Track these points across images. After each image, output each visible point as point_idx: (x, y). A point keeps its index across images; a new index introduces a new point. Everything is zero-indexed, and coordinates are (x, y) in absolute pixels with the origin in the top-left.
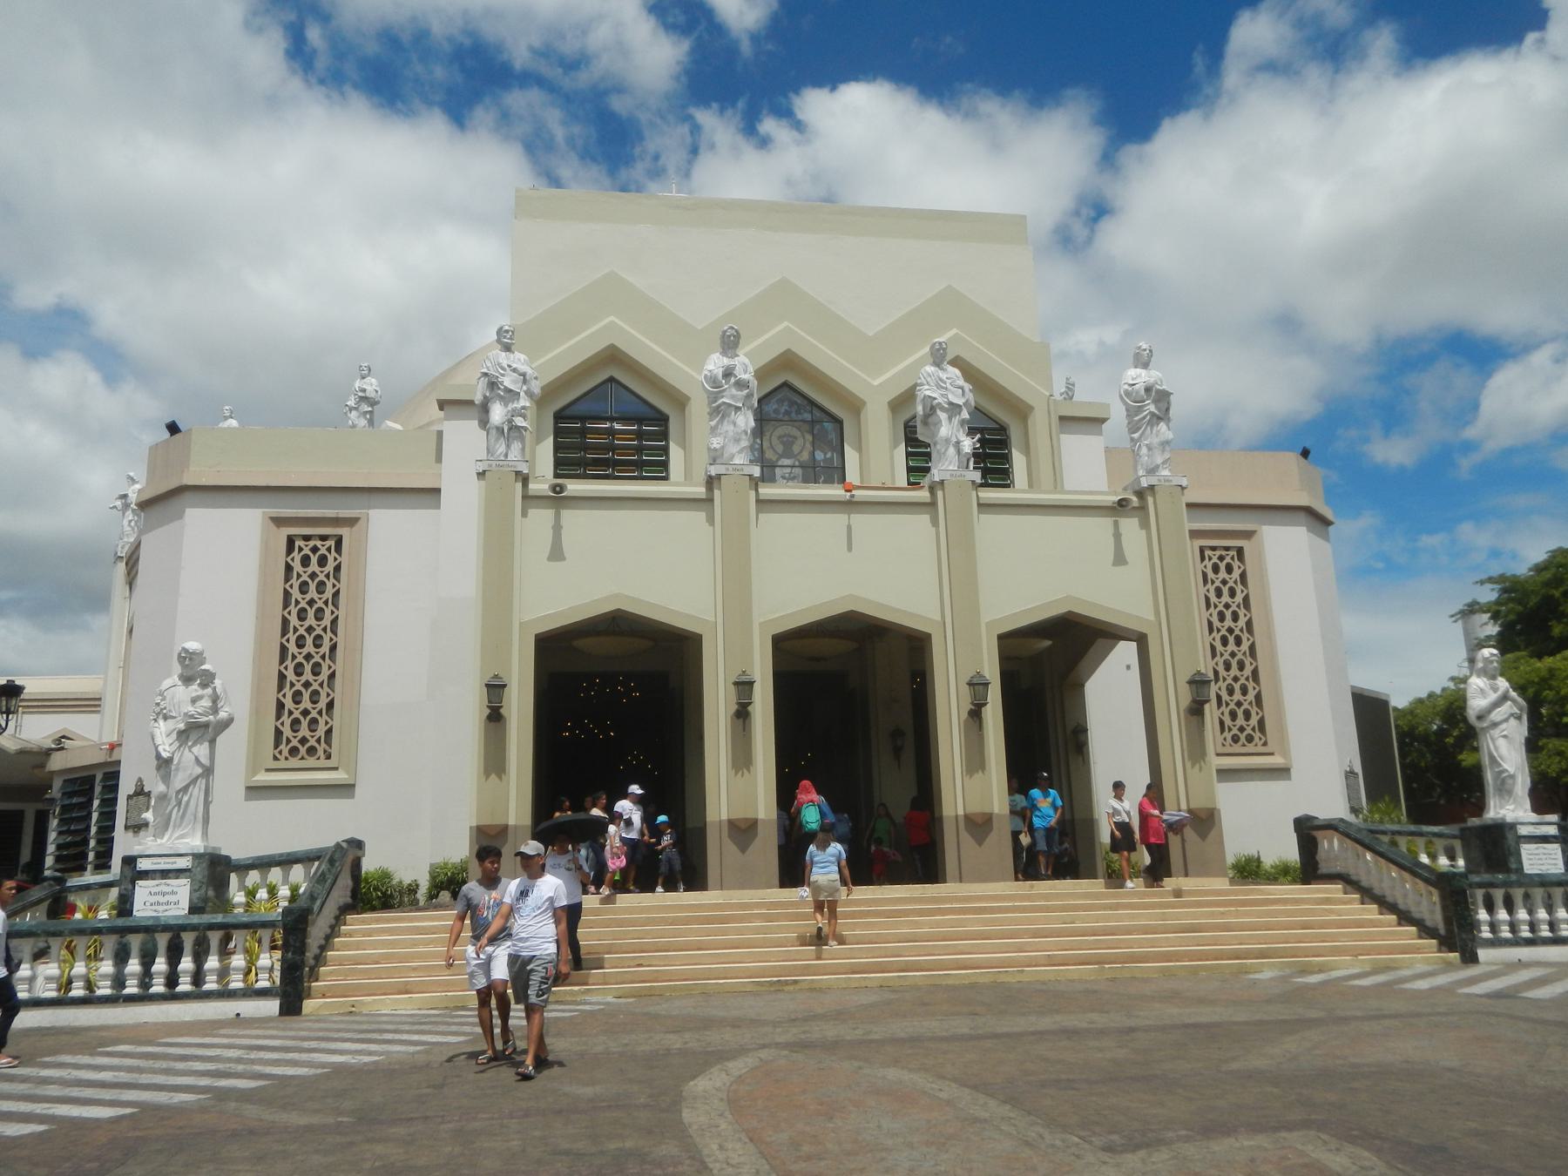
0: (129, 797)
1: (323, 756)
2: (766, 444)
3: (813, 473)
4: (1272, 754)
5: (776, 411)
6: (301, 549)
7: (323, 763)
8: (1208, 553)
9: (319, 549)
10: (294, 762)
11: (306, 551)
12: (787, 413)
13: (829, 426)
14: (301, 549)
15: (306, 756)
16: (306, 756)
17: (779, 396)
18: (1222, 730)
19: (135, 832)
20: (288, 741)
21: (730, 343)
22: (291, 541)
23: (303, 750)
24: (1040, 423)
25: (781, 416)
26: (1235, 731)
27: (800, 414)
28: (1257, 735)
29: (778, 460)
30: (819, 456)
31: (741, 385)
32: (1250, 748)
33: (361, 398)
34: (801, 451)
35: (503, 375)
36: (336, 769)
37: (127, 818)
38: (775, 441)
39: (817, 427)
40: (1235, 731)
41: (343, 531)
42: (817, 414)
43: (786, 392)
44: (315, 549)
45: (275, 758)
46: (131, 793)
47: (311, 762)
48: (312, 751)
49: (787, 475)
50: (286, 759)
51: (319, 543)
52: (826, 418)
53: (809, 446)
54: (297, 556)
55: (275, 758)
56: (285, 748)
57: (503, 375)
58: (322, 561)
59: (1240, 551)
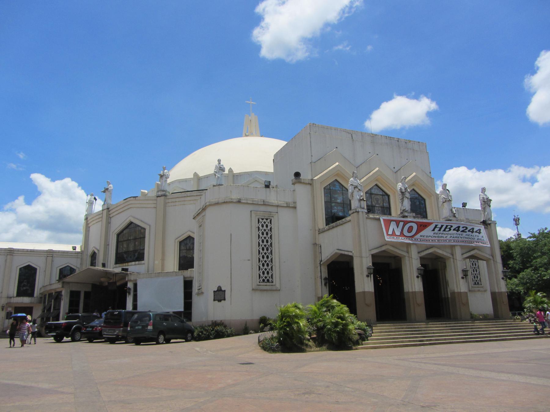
0: (214, 292)
2: (373, 201)
7: (271, 284)
13: (386, 197)
19: (218, 301)
23: (266, 280)
28: (479, 282)
29: (376, 205)
30: (385, 204)
37: (214, 298)
38: (375, 200)
39: (384, 197)
44: (265, 223)
46: (216, 289)
47: (268, 284)
49: (378, 209)
50: (262, 282)
51: (265, 220)
53: (382, 202)
55: (259, 282)
56: (262, 280)
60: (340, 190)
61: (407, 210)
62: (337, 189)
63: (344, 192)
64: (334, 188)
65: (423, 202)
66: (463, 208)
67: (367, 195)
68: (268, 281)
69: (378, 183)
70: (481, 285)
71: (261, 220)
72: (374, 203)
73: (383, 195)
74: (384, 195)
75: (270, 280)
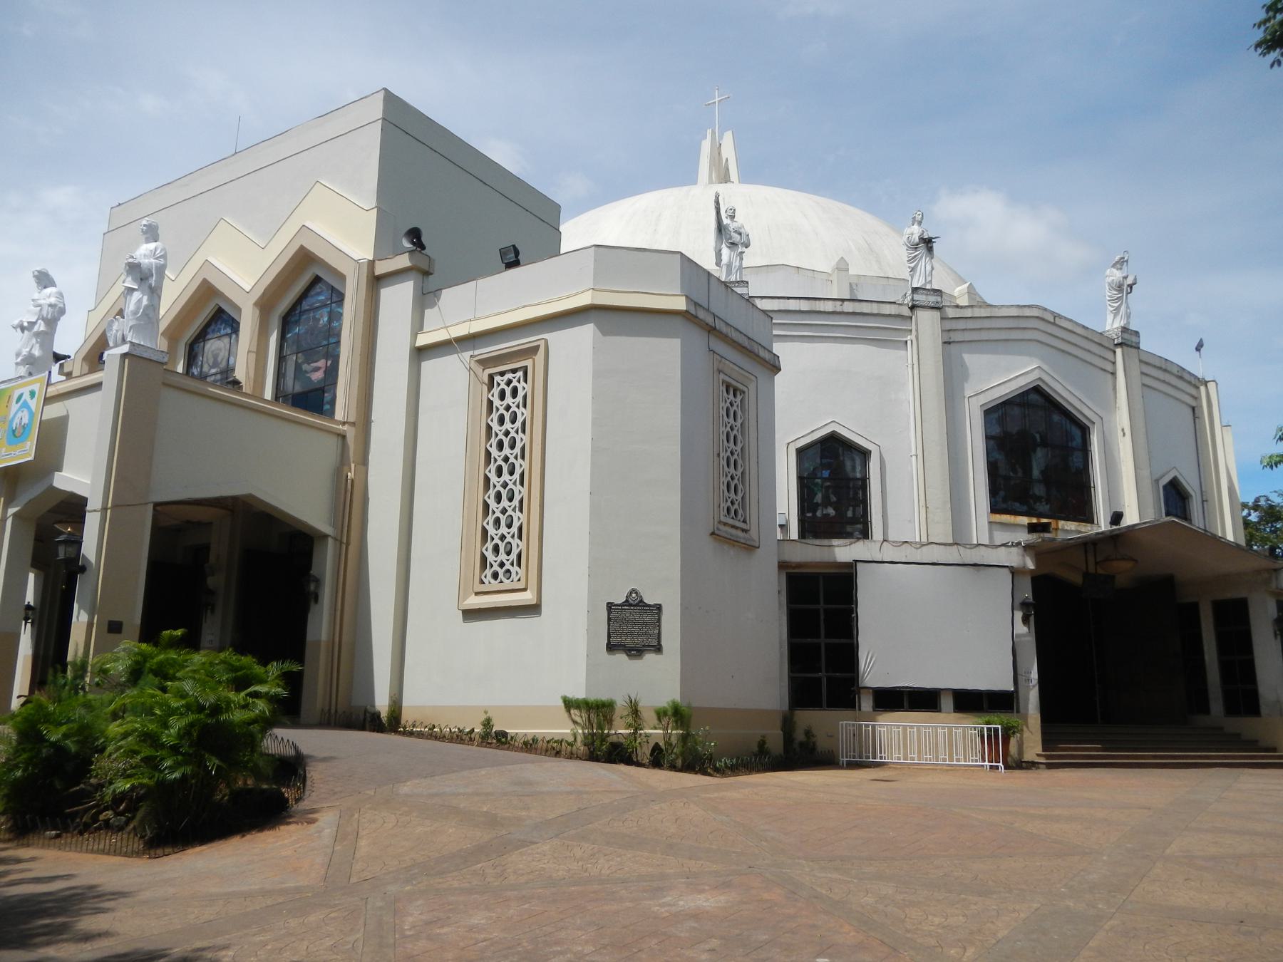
6: (499, 384)
10: (495, 585)
14: (499, 384)
36: (525, 590)
41: (528, 363)
47: (507, 584)
51: (510, 376)
54: (496, 391)
56: (489, 572)
58: (515, 392)
71: (498, 378)
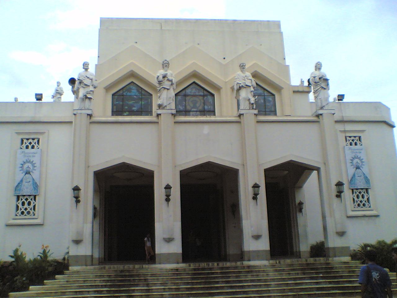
1: (32, 215)
3: (203, 112)
4: (373, 210)
5: (190, 92)
8: (348, 138)
9: (32, 143)
10: (23, 217)
11: (28, 144)
12: (195, 93)
13: (210, 98)
14: (26, 143)
15: (27, 214)
16: (27, 214)
17: (191, 86)
18: (354, 202)
20: (21, 209)
21: (166, 65)
22: (22, 141)
24: (286, 93)
25: (192, 94)
26: (359, 202)
27: (199, 93)
28: (367, 204)
29: (191, 109)
31: (168, 80)
32: (364, 208)
33: (57, 93)
34: (200, 106)
35: (84, 80)
39: (205, 98)
40: (359, 202)
42: (206, 93)
43: (194, 85)
45: (16, 215)
47: (28, 216)
48: (29, 213)
50: (20, 215)
52: (209, 94)
53: (202, 105)
56: (19, 212)
57: (84, 80)
59: (360, 137)
60: (138, 95)
61: (166, 106)
62: (133, 94)
63: (143, 96)
64: (129, 94)
65: (270, 99)
66: (339, 101)
67: (179, 97)
68: (29, 213)
69: (195, 81)
70: (370, 207)
71: (25, 141)
72: (188, 108)
73: (204, 96)
74: (206, 95)
75: (31, 212)
